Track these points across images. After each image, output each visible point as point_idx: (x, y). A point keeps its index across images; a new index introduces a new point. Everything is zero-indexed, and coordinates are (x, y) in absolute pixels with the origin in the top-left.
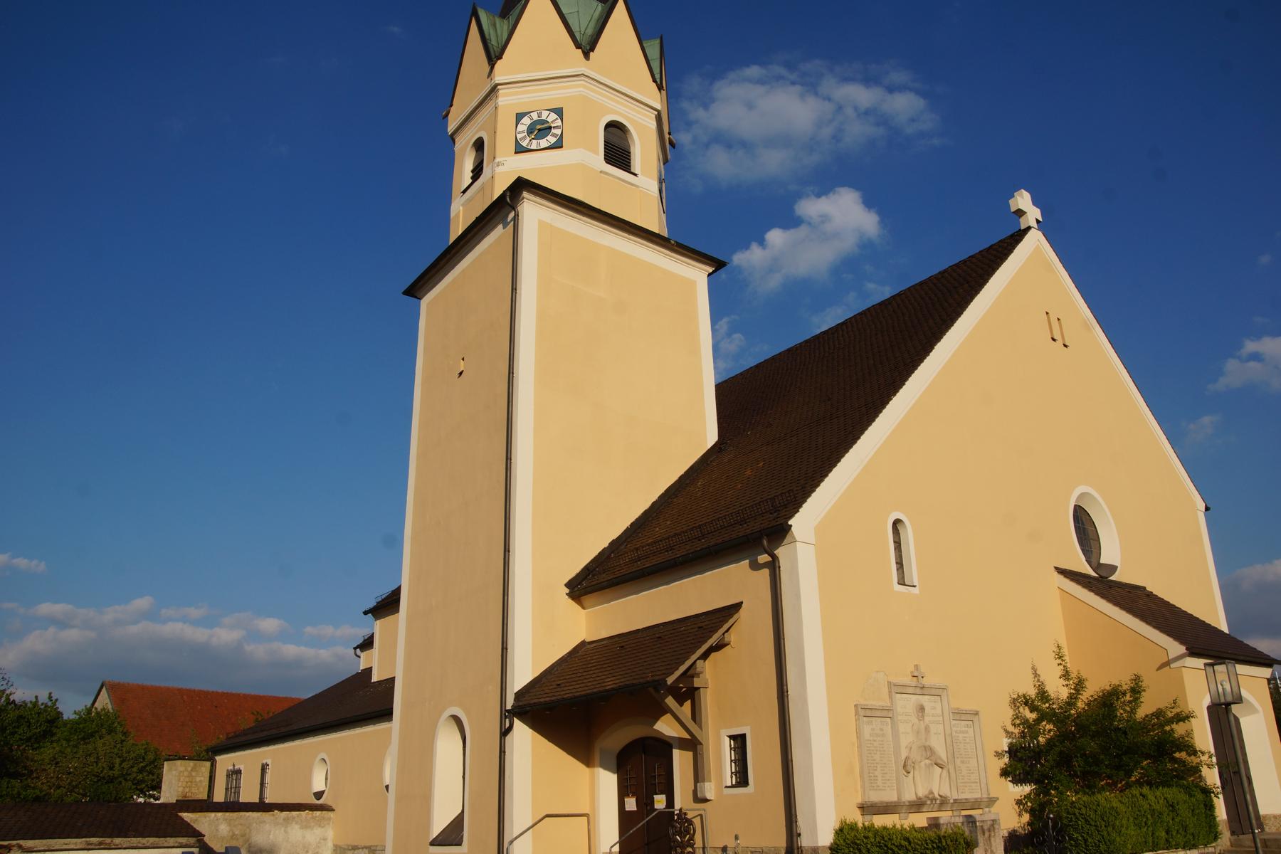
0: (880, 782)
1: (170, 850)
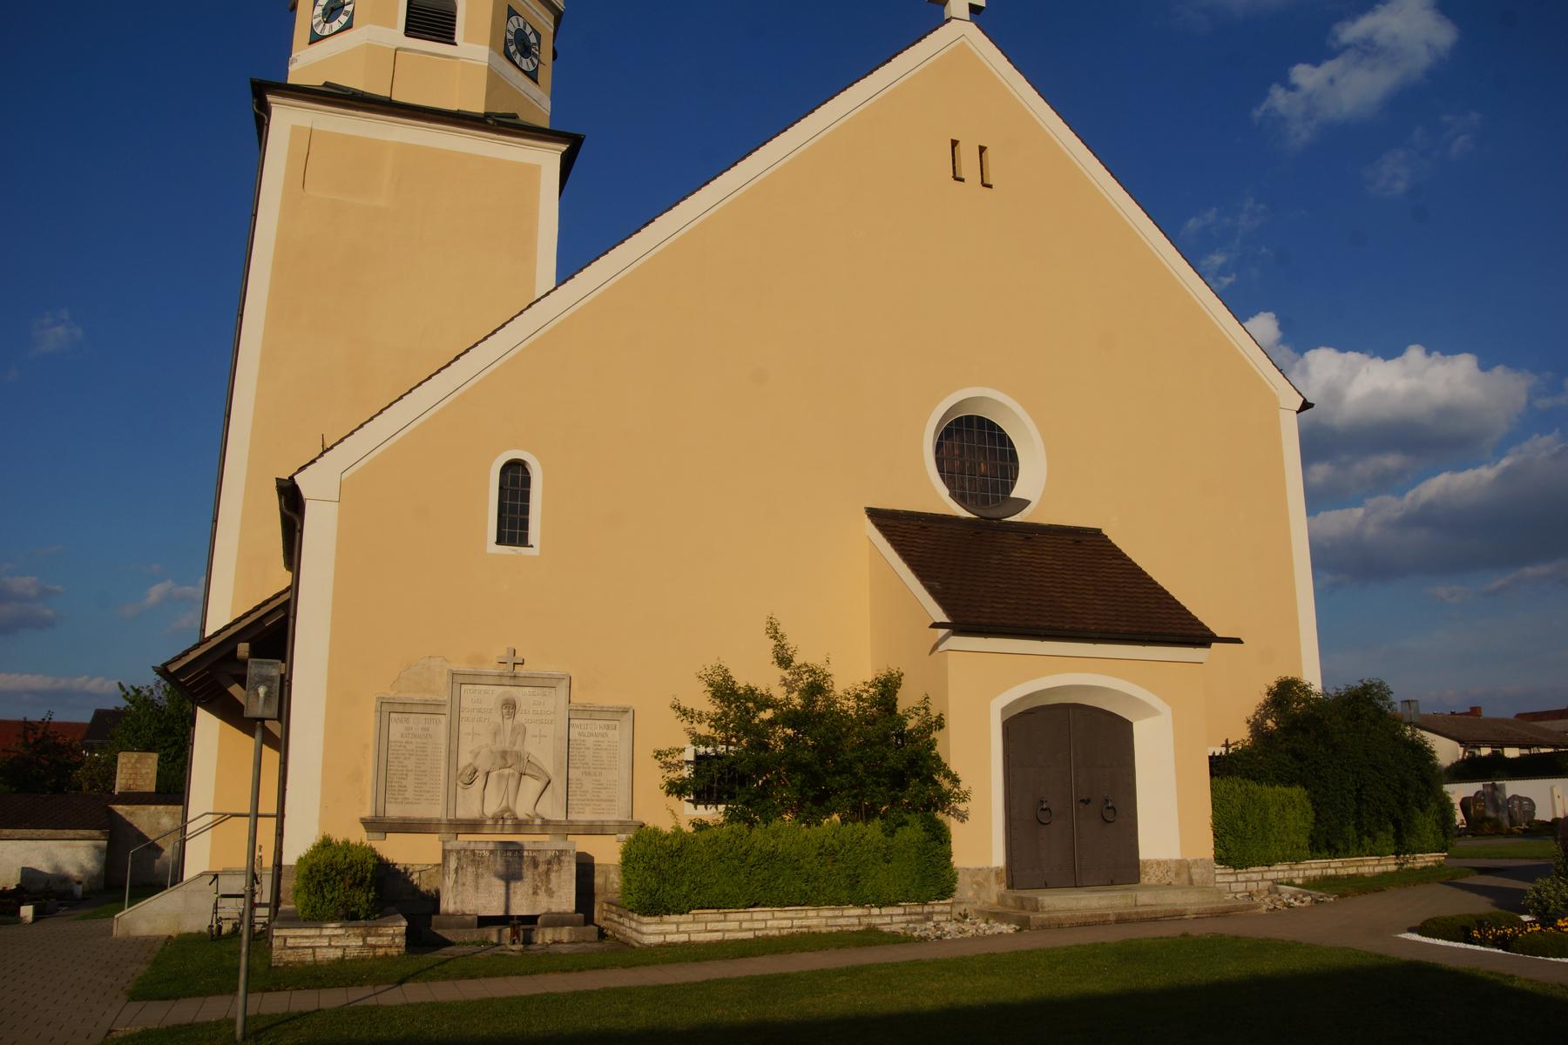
0: (410, 794)
1: (73, 842)
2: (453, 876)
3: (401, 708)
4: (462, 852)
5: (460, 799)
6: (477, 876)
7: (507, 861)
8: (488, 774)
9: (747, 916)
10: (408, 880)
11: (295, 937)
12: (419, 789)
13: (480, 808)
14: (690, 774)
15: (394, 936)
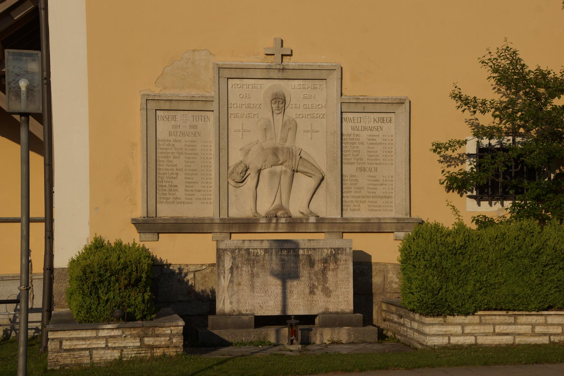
0: (181, 193)
2: (228, 275)
3: (167, 106)
4: (237, 251)
5: (232, 198)
6: (253, 275)
7: (282, 260)
8: (259, 171)
9: (541, 319)
10: (183, 281)
11: (71, 339)
12: (190, 189)
13: (253, 208)
14: (472, 168)
15: (171, 336)
